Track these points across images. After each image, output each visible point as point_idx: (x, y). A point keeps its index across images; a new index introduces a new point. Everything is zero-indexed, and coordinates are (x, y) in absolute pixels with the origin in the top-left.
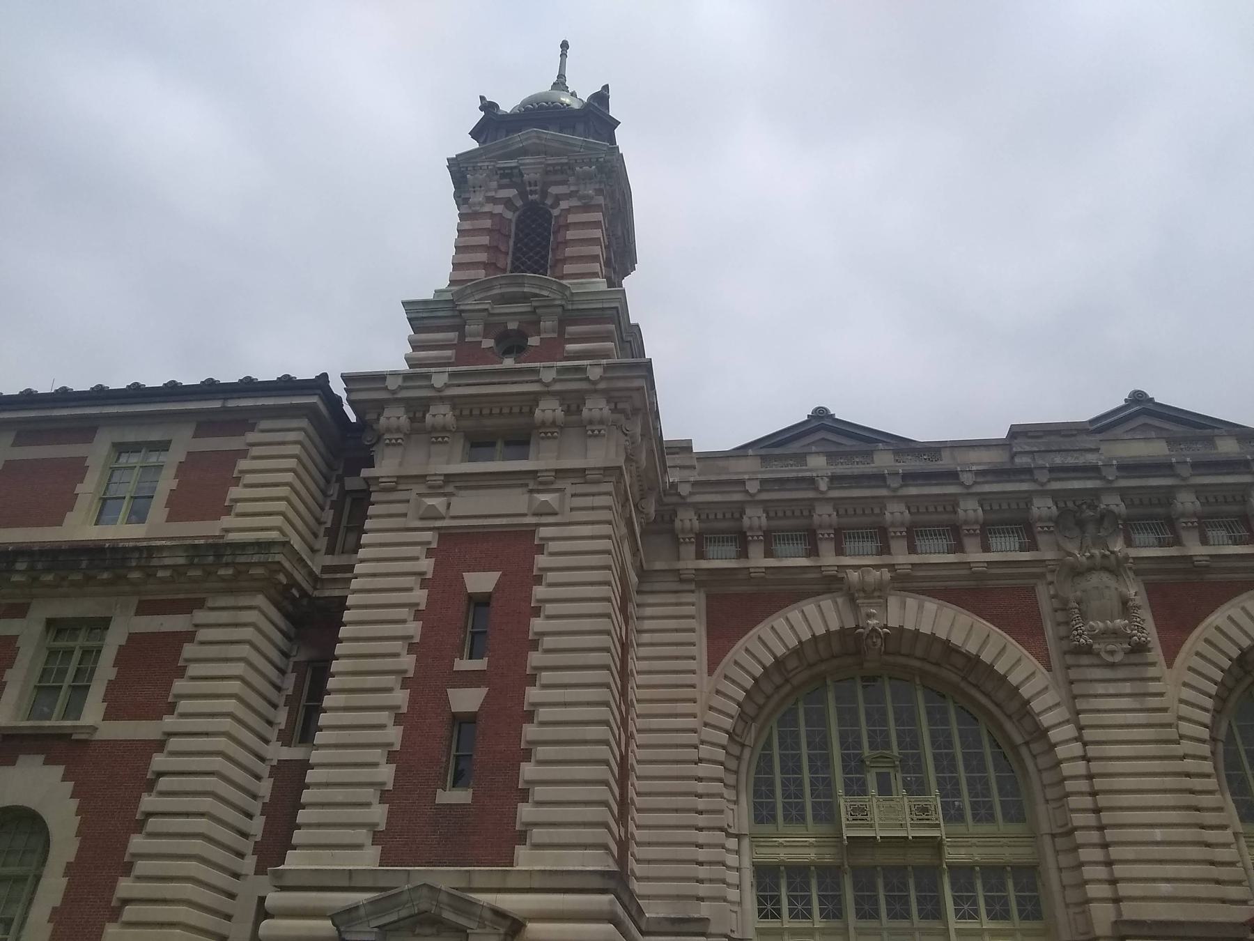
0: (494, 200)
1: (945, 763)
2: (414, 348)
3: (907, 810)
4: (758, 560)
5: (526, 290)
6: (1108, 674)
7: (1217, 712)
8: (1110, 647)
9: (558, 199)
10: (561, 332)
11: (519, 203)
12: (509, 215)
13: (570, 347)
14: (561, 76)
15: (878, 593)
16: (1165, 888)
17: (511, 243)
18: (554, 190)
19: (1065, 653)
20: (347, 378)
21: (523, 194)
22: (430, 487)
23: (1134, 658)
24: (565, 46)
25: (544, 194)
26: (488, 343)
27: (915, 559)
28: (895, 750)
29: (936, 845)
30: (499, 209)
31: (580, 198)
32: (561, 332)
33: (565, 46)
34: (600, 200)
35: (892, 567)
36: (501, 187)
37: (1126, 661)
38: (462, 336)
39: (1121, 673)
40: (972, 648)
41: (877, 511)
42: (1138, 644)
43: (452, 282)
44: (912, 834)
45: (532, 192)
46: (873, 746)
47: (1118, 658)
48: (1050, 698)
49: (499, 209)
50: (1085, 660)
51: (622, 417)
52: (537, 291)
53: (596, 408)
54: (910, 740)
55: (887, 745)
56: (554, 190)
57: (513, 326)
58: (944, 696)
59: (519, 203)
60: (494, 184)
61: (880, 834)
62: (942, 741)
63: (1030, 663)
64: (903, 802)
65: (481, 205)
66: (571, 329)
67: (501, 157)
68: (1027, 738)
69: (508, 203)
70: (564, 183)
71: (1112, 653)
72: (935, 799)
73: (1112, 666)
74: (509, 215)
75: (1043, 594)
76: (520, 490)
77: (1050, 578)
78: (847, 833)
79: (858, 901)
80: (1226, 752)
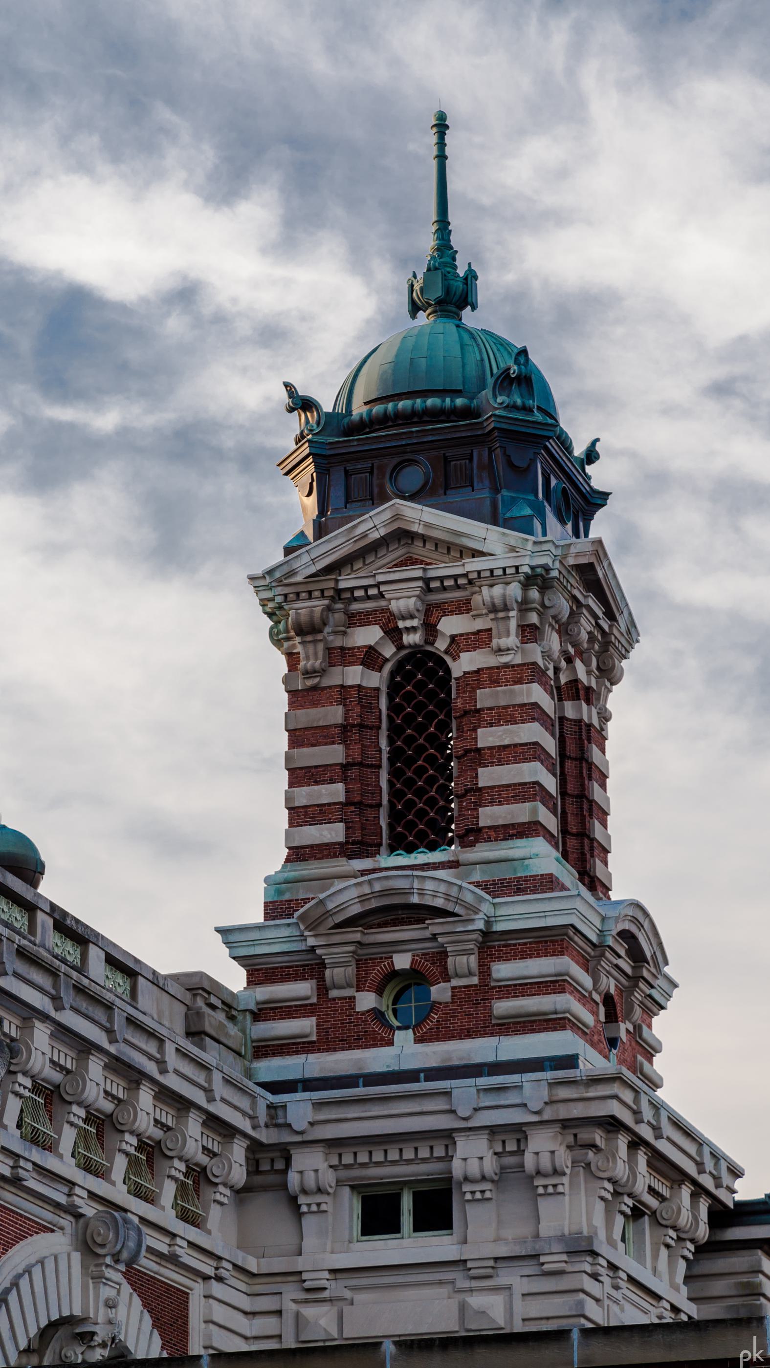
9: (458, 643)
10: (485, 972)
11: (388, 651)
12: (376, 680)
13: (502, 1007)
18: (451, 625)
21: (393, 633)
22: (308, 1290)
25: (431, 630)
26: (366, 1001)
32: (485, 972)
38: (322, 989)
43: (298, 854)
53: (544, 1147)
56: (451, 625)
57: (402, 962)
59: (388, 651)
65: (321, 672)
70: (463, 607)
74: (376, 680)
76: (444, 1291)
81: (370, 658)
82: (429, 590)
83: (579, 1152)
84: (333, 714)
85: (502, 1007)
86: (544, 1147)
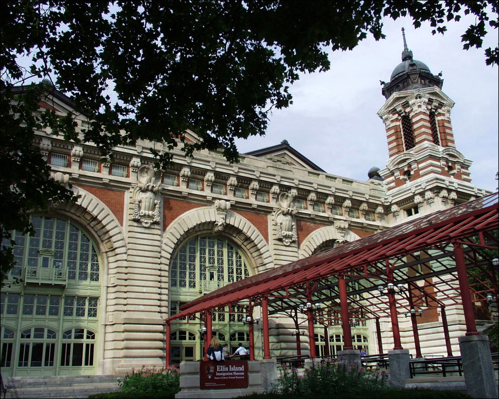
1: (72, 257)
3: (54, 274)
6: (143, 230)
7: (175, 249)
8: (146, 221)
16: (142, 308)
19: (130, 220)
27: (82, 172)
28: (53, 249)
29: (63, 287)
35: (70, 174)
39: (147, 231)
40: (95, 213)
41: (70, 148)
42: (156, 221)
44: (53, 282)
46: (44, 246)
47: (147, 225)
48: (119, 237)
50: (135, 224)
54: (60, 245)
55: (50, 246)
58: (78, 229)
61: (40, 282)
62: (73, 247)
63: (116, 222)
64: (51, 270)
68: (107, 250)
71: (146, 223)
72: (66, 269)
73: (145, 228)
75: (127, 195)
77: (131, 190)
78: (27, 281)
79: (25, 308)
80: (174, 263)
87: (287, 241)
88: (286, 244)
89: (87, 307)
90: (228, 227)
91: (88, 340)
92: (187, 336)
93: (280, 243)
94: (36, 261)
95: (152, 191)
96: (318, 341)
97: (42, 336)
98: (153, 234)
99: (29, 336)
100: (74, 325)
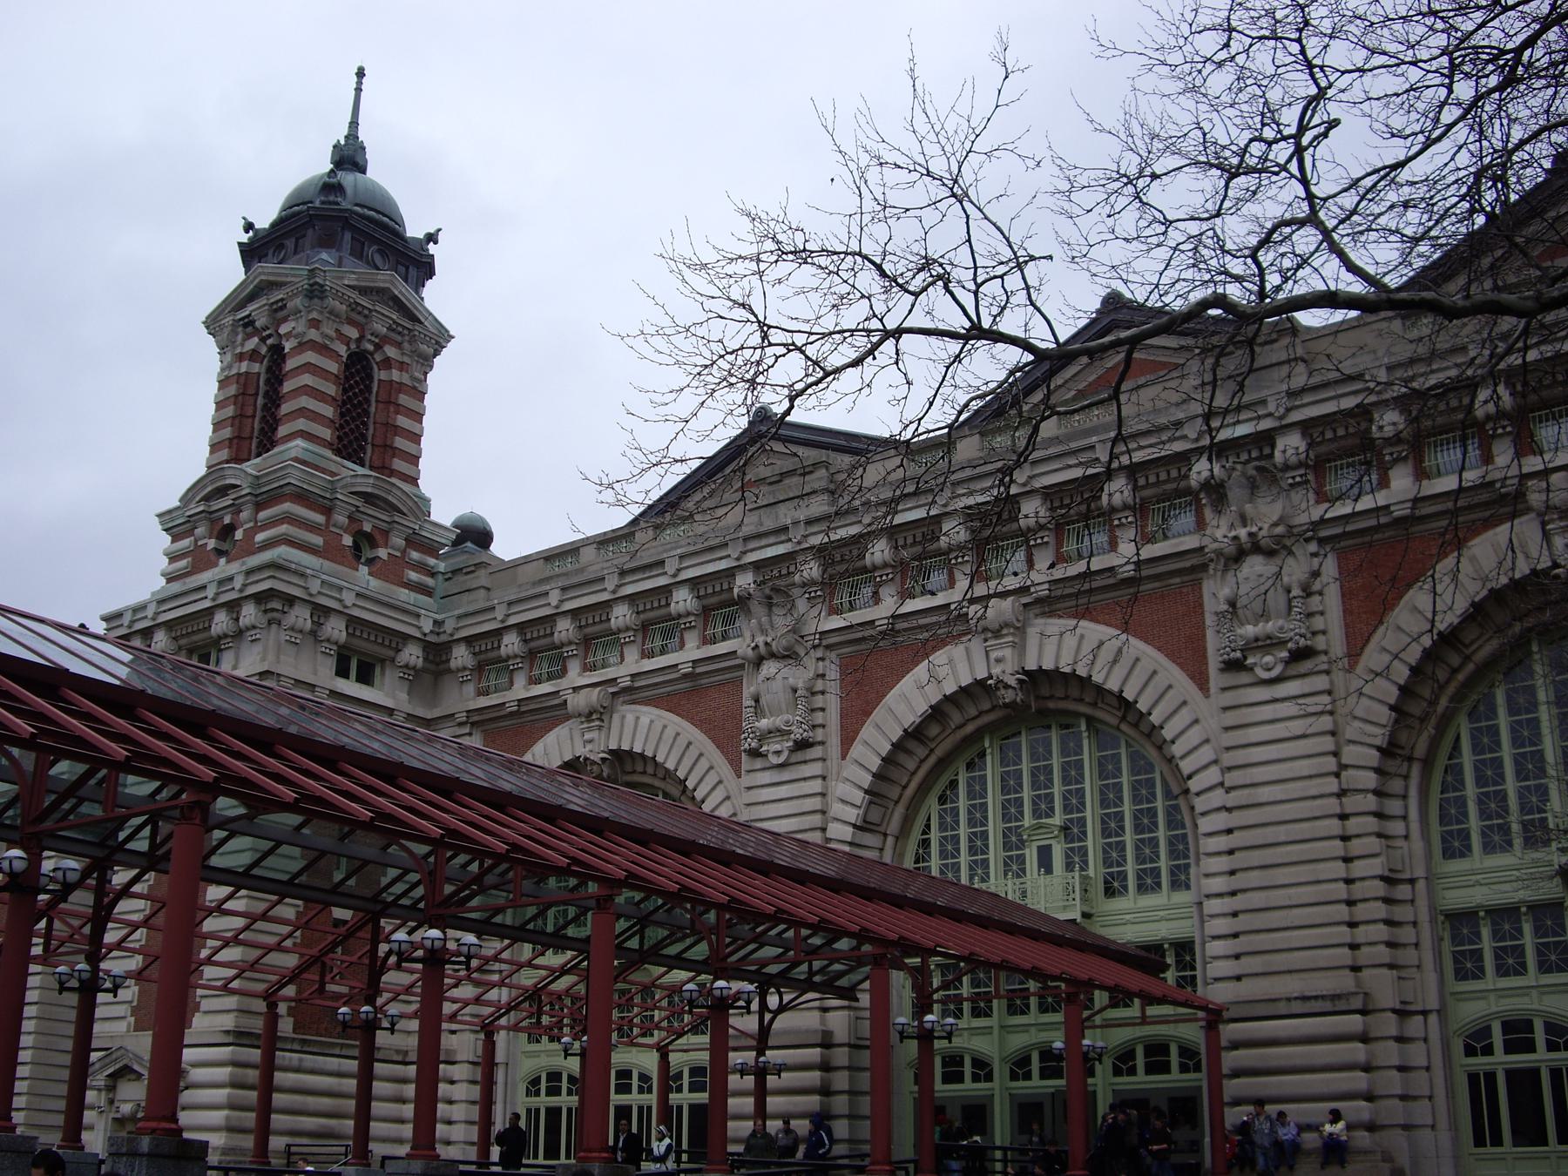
0: (240, 357)
2: (173, 558)
4: (521, 689)
5: (228, 482)
6: (767, 777)
8: (778, 747)
12: (256, 368)
13: (260, 537)
14: (354, 124)
15: (597, 716)
17: (260, 401)
20: (106, 619)
23: (799, 756)
24: (361, 73)
30: (244, 367)
31: (296, 337)
33: (361, 73)
34: (313, 334)
36: (248, 337)
37: (793, 760)
39: (786, 775)
45: (269, 336)
47: (781, 760)
49: (244, 367)
51: (275, 615)
52: (233, 481)
57: (227, 520)
60: (240, 337)
66: (262, 515)
67: (242, 305)
69: (254, 355)
71: (778, 753)
74: (256, 368)
81: (254, 355)
82: (276, 311)
83: (270, 615)
84: (232, 390)
85: (260, 537)
86: (249, 613)
87: (1267, 663)
88: (1265, 675)
89: (1487, 944)
90: (1034, 679)
91: (1472, 1060)
92: (968, 1069)
93: (1244, 678)
94: (1021, 860)
95: (773, 655)
96: (679, 1090)
97: (1530, 1047)
98: (805, 779)
99: (1488, 1050)
100: (1494, 1009)
